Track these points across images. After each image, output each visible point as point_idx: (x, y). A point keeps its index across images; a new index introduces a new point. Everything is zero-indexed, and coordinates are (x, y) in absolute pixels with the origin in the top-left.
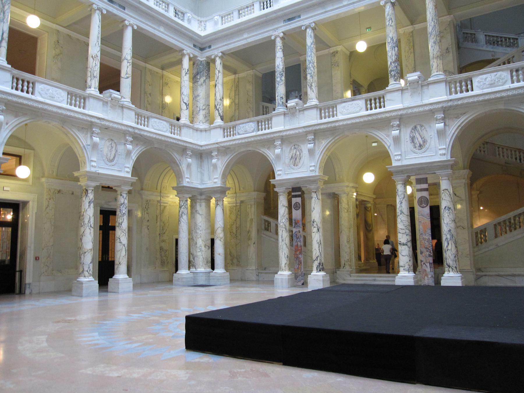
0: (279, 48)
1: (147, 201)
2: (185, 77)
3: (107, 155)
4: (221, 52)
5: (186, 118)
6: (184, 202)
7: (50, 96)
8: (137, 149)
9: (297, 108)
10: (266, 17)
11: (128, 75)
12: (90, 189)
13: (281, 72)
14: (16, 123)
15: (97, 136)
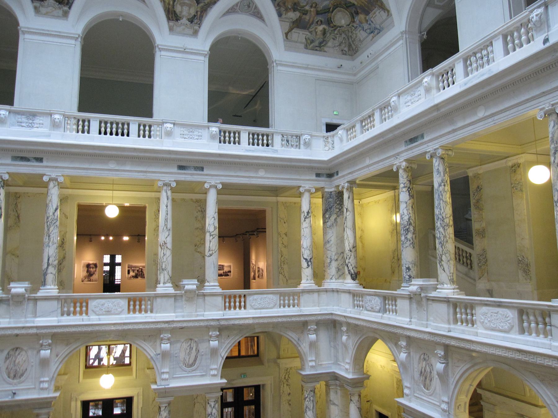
0: (402, 185)
1: (287, 370)
2: (304, 223)
3: (185, 359)
4: (348, 182)
5: (307, 280)
6: (308, 393)
7: (105, 311)
8: (228, 342)
9: (423, 295)
10: (383, 138)
11: (211, 252)
12: (162, 406)
13: (405, 227)
14: (66, 353)
15: (168, 342)
